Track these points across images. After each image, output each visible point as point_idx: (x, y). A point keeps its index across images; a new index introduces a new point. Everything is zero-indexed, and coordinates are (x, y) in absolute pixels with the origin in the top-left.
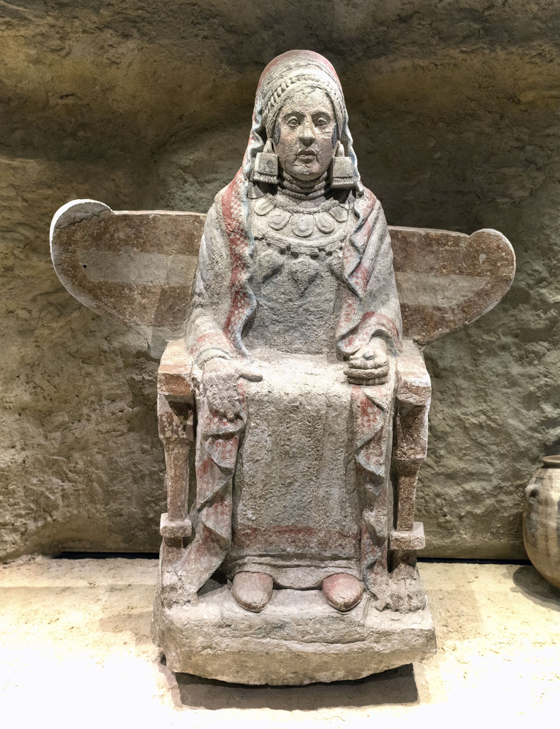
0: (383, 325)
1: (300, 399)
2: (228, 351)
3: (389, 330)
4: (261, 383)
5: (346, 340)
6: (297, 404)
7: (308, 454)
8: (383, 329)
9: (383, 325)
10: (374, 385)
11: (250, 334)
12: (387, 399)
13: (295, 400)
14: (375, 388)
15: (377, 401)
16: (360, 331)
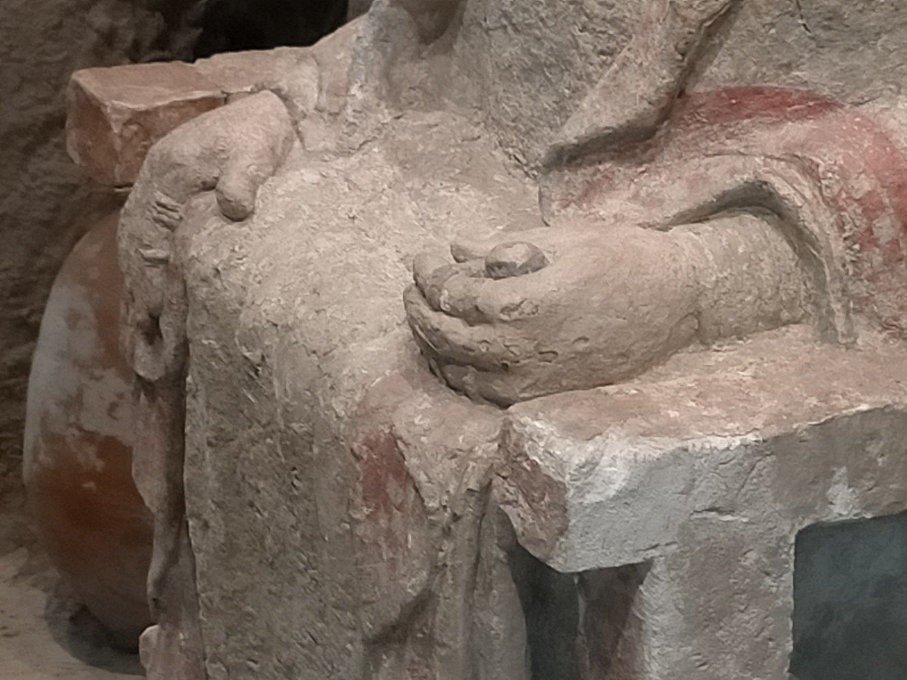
0: (810, 171)
1: (271, 341)
2: (326, 85)
3: (833, 204)
4: (233, 227)
5: (579, 177)
6: (254, 356)
7: (299, 578)
8: (791, 188)
9: (810, 171)
10: (458, 389)
11: (457, 47)
12: (459, 474)
13: (252, 338)
14: (458, 406)
15: (412, 462)
16: (667, 157)
